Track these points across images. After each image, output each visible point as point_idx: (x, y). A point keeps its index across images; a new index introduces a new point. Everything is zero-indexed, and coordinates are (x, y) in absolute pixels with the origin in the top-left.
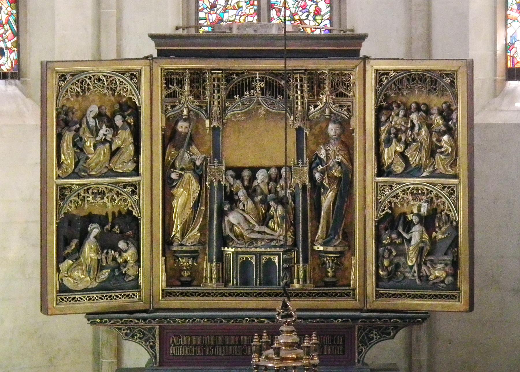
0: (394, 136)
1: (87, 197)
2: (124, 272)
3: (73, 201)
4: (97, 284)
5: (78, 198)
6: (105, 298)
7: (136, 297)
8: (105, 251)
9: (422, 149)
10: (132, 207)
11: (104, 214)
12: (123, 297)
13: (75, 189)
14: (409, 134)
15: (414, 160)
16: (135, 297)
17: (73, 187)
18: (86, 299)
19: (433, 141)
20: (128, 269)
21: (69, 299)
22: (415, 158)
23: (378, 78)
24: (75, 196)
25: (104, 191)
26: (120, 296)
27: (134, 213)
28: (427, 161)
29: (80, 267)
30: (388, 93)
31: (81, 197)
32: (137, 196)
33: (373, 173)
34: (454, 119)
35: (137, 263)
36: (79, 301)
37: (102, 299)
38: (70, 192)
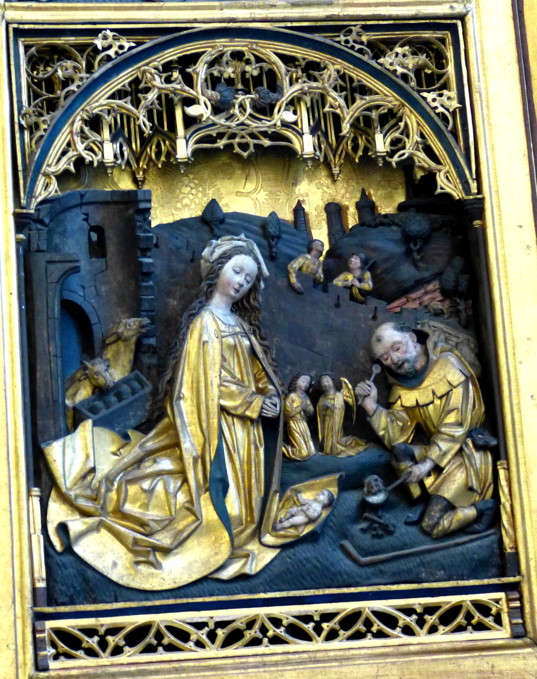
1: (190, 101)
2: (416, 491)
3: (109, 119)
4: (269, 555)
5: (136, 103)
6: (318, 630)
7: (498, 620)
8: (303, 381)
10: (429, 151)
11: (287, 215)
12: (421, 623)
13: (111, 52)
16: (489, 621)
17: (99, 43)
18: (212, 636)
20: (437, 470)
21: (110, 639)
24: (119, 94)
25: (272, 76)
26: (403, 619)
27: (441, 179)
29: (166, 464)
31: (152, 96)
32: (453, 94)
35: (481, 438)
36: (171, 648)
37: (307, 637)
38: (90, 69)
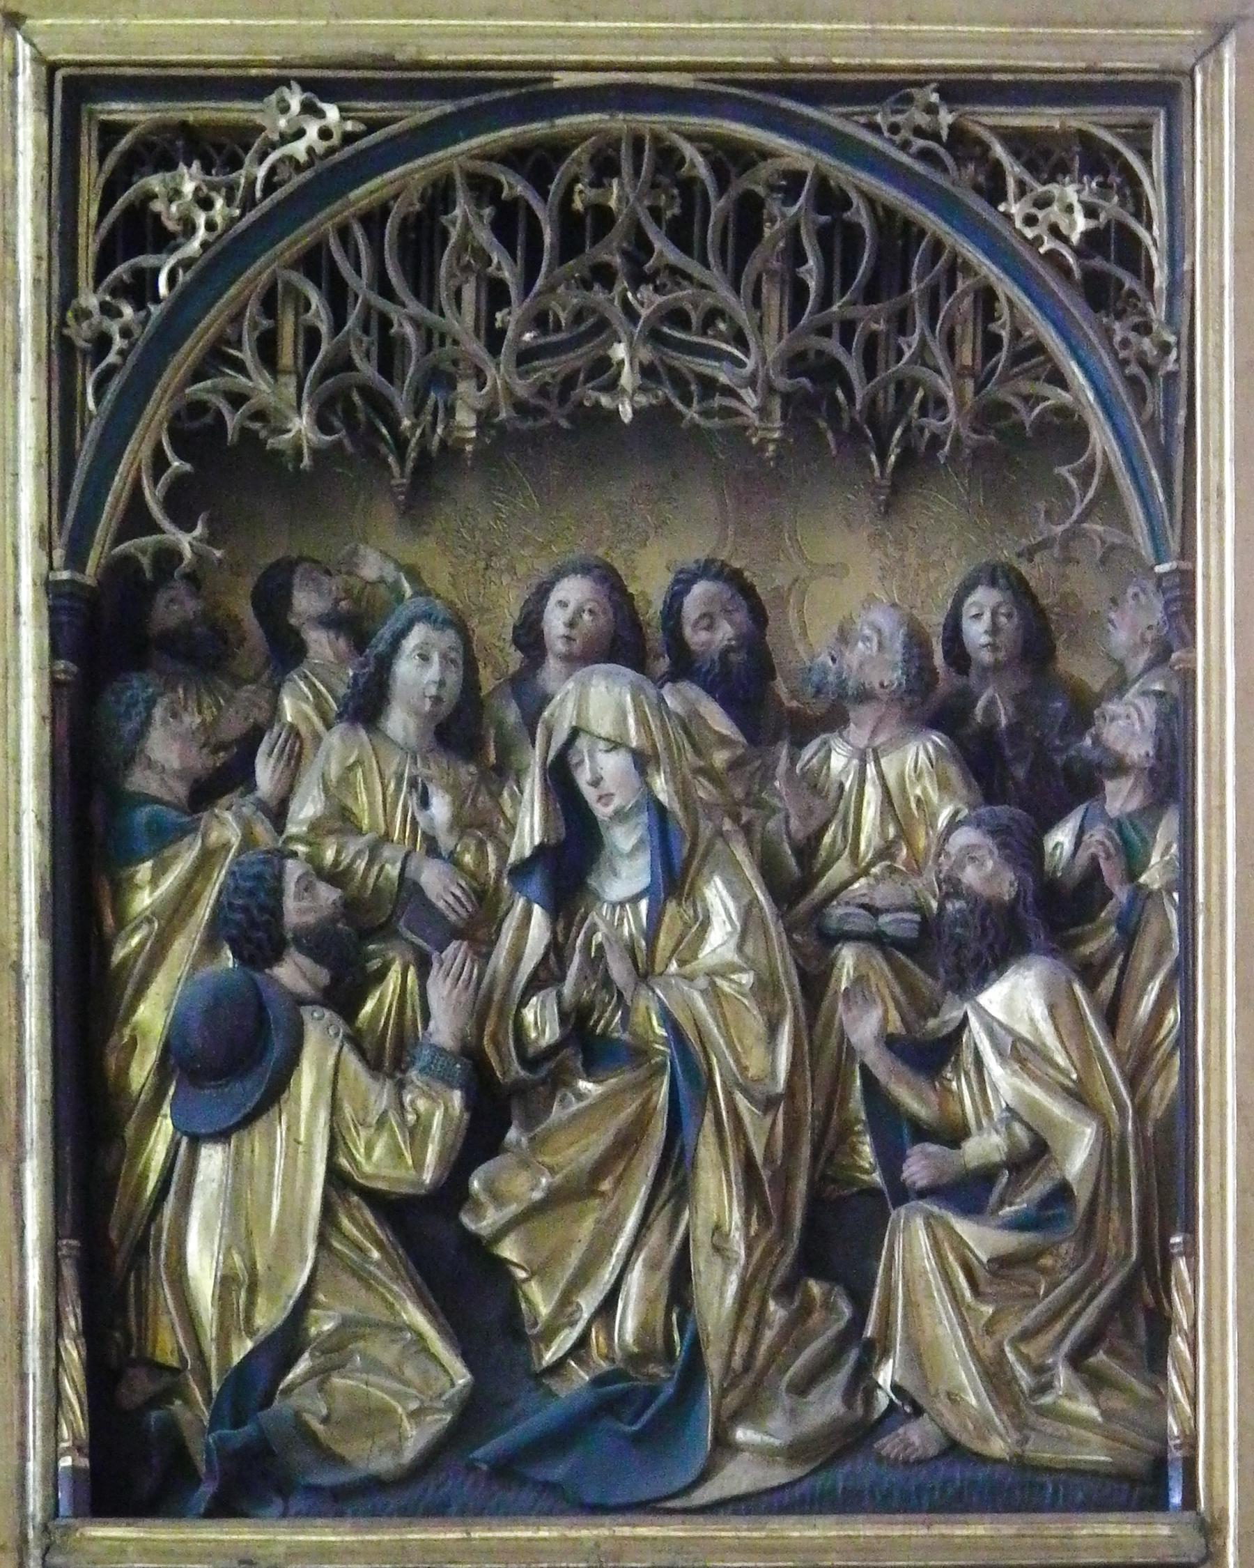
0: (323, 976)
9: (707, 1152)
14: (516, 956)
15: (588, 1303)
19: (847, 1052)
22: (607, 1275)
23: (89, 209)
28: (761, 1320)
30: (237, 399)
33: (33, 1468)
34: (1119, 768)
